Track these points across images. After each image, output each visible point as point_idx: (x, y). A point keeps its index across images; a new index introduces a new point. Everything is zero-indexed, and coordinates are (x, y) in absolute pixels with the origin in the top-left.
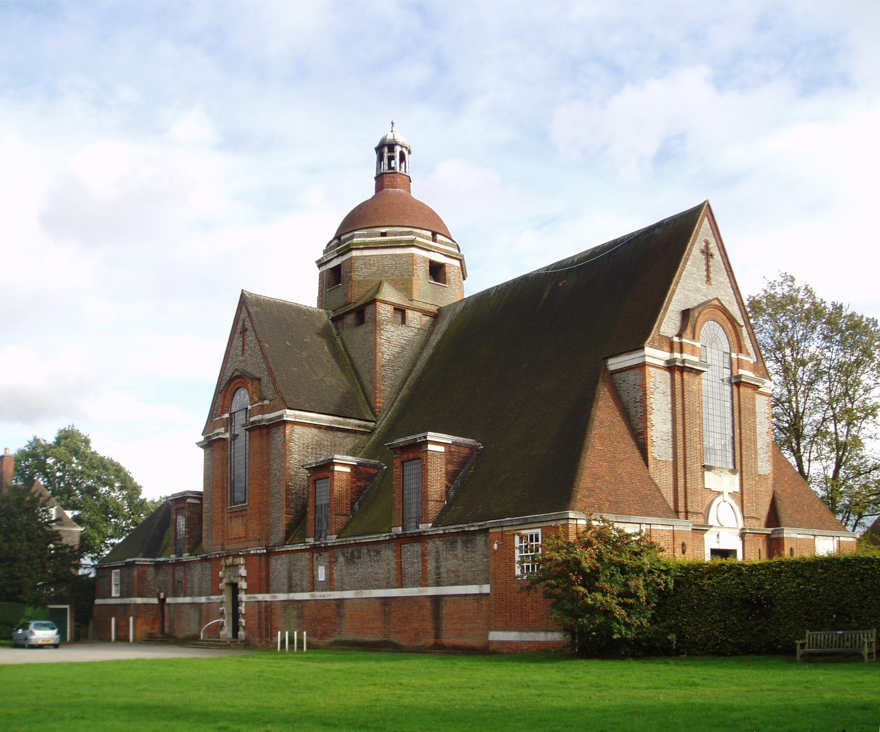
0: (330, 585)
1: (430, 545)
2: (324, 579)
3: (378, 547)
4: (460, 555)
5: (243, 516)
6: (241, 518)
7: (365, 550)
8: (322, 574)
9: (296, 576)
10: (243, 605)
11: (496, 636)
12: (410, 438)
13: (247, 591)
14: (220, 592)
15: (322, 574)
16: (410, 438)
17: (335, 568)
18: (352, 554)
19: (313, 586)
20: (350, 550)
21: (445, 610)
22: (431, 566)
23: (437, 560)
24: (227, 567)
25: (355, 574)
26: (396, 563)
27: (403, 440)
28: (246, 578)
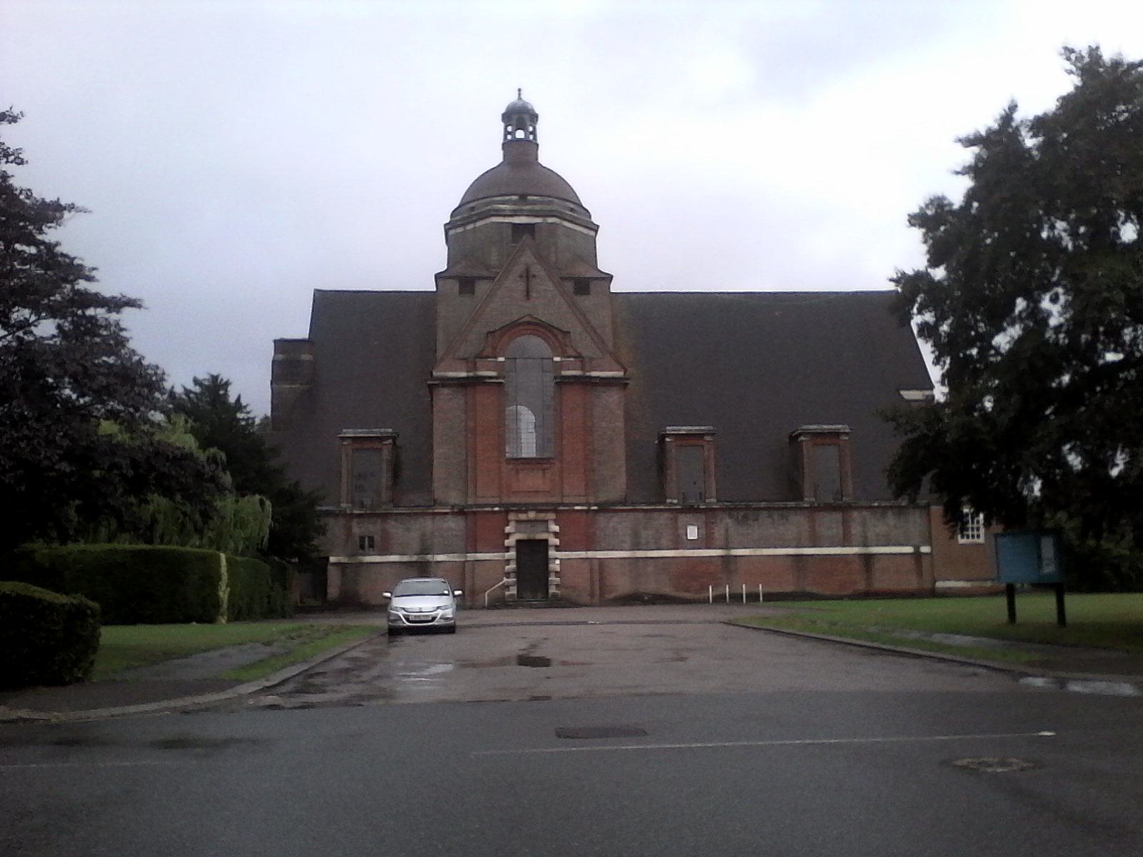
0: (705, 541)
1: (855, 514)
2: (696, 538)
3: (785, 513)
4: (892, 523)
5: (544, 470)
6: (541, 474)
7: (765, 513)
8: (693, 533)
9: (646, 535)
10: (558, 562)
11: (940, 584)
12: (825, 427)
13: (558, 548)
14: (507, 549)
15: (693, 533)
16: (833, 427)
17: (716, 528)
18: (745, 517)
19: (679, 542)
20: (742, 513)
21: (877, 565)
22: (856, 530)
23: (864, 524)
24: (518, 522)
25: (748, 534)
26: (810, 527)
27: (815, 427)
28: (556, 535)
